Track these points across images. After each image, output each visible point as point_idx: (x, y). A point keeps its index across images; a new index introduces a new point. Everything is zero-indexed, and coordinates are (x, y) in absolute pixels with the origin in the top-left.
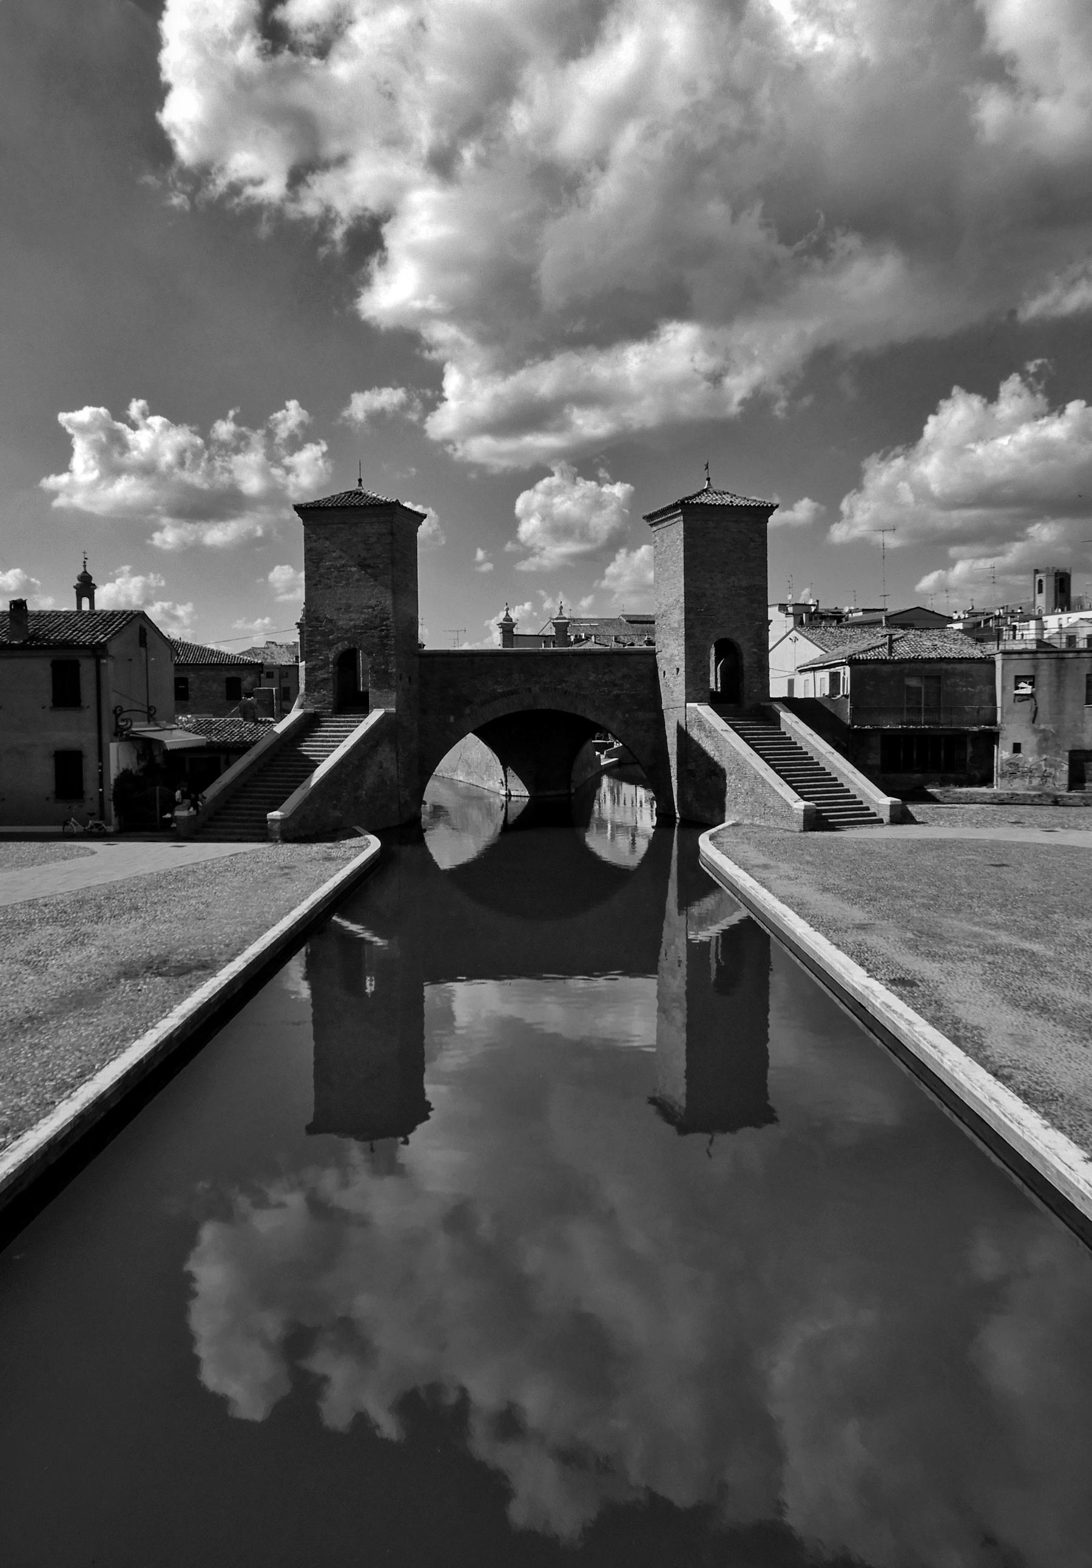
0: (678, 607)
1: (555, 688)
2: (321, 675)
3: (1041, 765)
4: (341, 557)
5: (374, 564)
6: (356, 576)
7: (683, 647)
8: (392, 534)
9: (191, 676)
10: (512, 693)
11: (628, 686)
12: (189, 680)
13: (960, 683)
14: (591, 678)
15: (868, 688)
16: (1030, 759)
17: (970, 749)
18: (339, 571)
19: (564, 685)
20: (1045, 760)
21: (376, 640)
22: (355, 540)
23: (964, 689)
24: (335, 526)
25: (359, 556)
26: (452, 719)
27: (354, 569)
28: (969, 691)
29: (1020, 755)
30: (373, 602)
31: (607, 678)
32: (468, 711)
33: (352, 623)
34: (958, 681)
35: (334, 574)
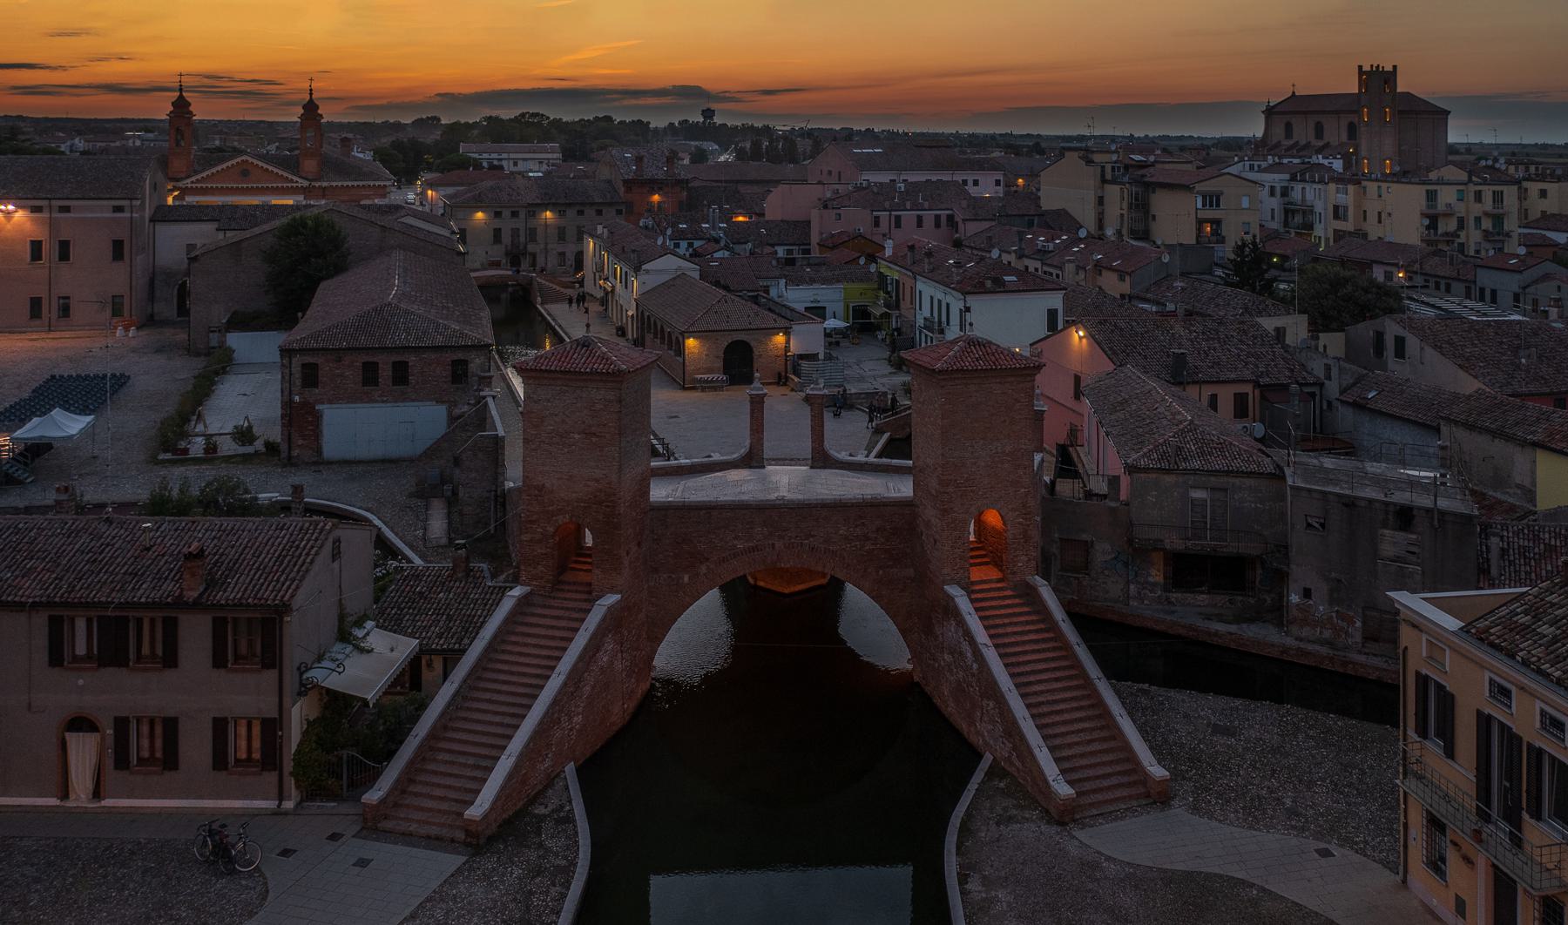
3: (1332, 617)
4: (563, 421)
8: (620, 402)
9: (412, 359)
10: (753, 549)
11: (883, 540)
12: (410, 364)
14: (841, 532)
16: (1321, 608)
19: (811, 539)
20: (1337, 611)
22: (579, 405)
25: (584, 422)
26: (686, 579)
27: (576, 436)
29: (1311, 602)
32: (703, 569)
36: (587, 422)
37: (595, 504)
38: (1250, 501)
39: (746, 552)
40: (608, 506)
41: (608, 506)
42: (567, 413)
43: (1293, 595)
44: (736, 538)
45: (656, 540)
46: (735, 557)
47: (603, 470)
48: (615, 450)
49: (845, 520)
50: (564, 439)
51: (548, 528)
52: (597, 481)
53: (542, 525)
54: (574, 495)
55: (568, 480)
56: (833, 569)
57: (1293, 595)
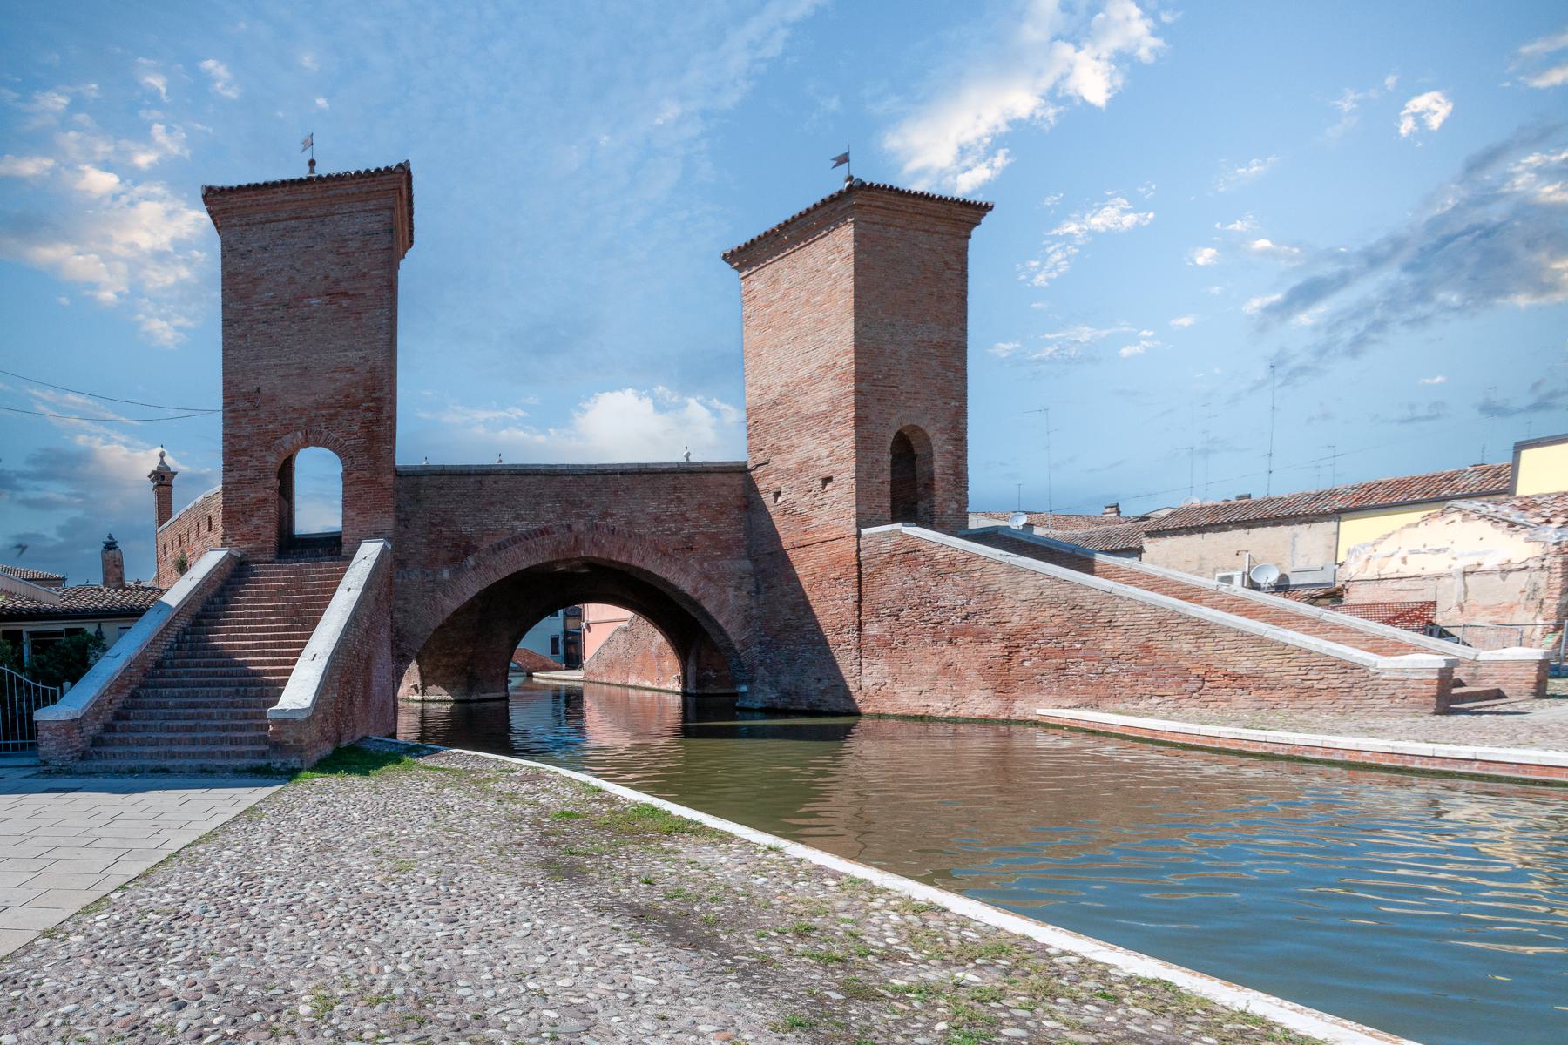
2: (252, 495)
7: (850, 441)
18: (287, 306)
21: (356, 428)
27: (315, 302)
30: (352, 357)
33: (312, 398)
35: (278, 314)
37: (345, 407)
40: (368, 409)
41: (368, 409)
47: (361, 350)
50: (291, 311)
51: (268, 458)
52: (350, 370)
53: (257, 454)
54: (312, 398)
55: (301, 375)
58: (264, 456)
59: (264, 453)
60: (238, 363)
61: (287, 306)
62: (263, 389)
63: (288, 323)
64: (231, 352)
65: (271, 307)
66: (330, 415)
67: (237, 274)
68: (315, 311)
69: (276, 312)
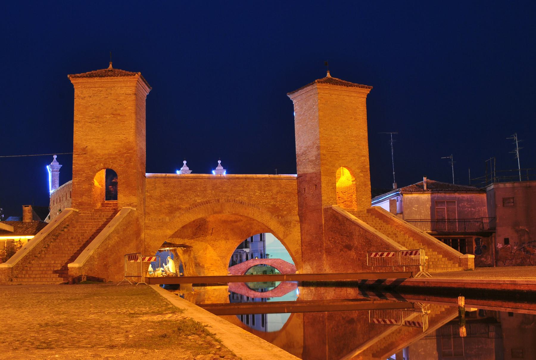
0: (315, 147)
1: (235, 200)
4: (100, 108)
5: (122, 113)
6: (110, 121)
10: (207, 202)
13: (467, 205)
15: (413, 208)
17: (474, 246)
19: (240, 198)
20: (524, 247)
22: (109, 98)
23: (470, 209)
24: (96, 89)
25: (112, 108)
27: (108, 116)
28: (473, 211)
29: (509, 246)
30: (122, 137)
31: (267, 194)
34: (465, 204)
36: (114, 107)
38: (468, 208)
39: (202, 204)
42: (102, 103)
43: (499, 244)
44: (198, 196)
45: (149, 196)
46: (196, 207)
47: (124, 135)
48: (132, 122)
49: (259, 187)
50: (99, 119)
51: (90, 173)
56: (253, 215)
57: (499, 244)
58: (89, 172)
59: (88, 171)
60: (79, 137)
61: (98, 117)
62: (89, 147)
63: (98, 123)
64: (77, 133)
65: (92, 117)
66: (113, 158)
67: (80, 105)
68: (108, 120)
69: (94, 119)
